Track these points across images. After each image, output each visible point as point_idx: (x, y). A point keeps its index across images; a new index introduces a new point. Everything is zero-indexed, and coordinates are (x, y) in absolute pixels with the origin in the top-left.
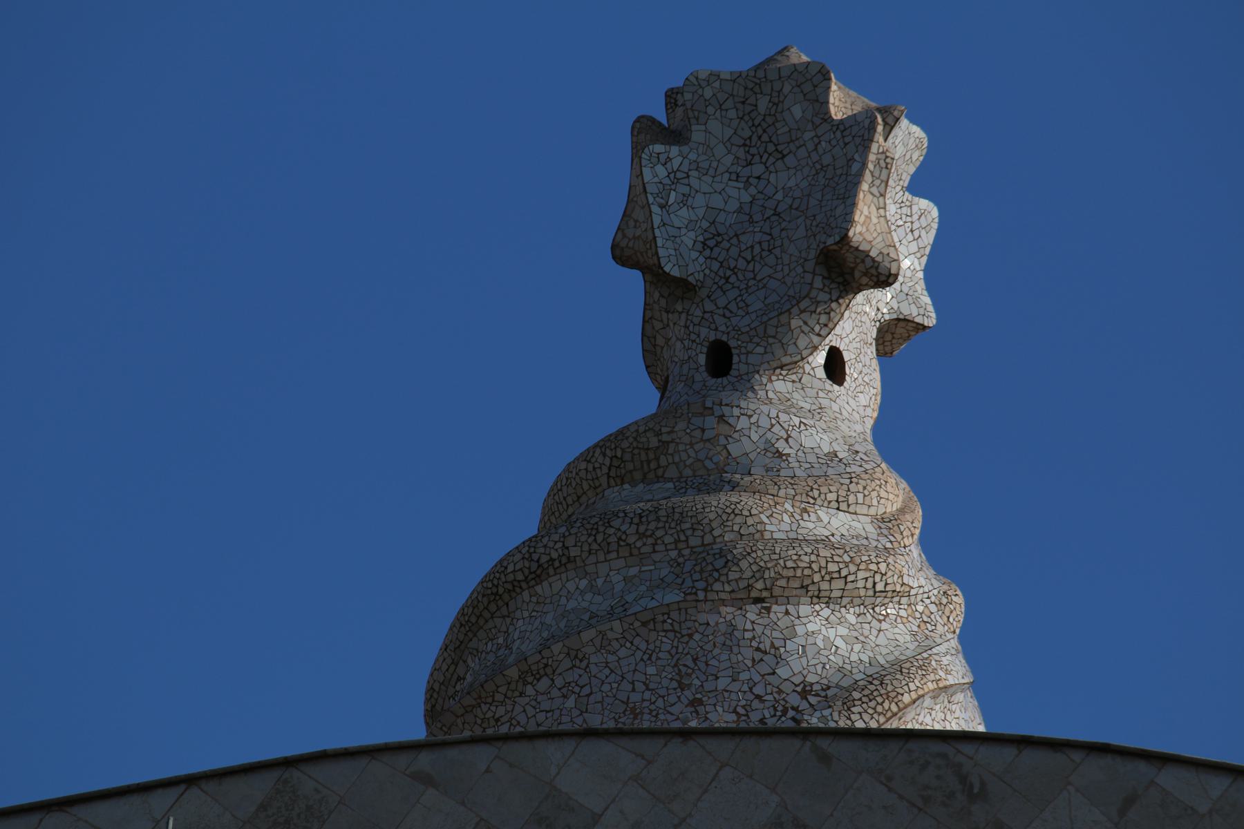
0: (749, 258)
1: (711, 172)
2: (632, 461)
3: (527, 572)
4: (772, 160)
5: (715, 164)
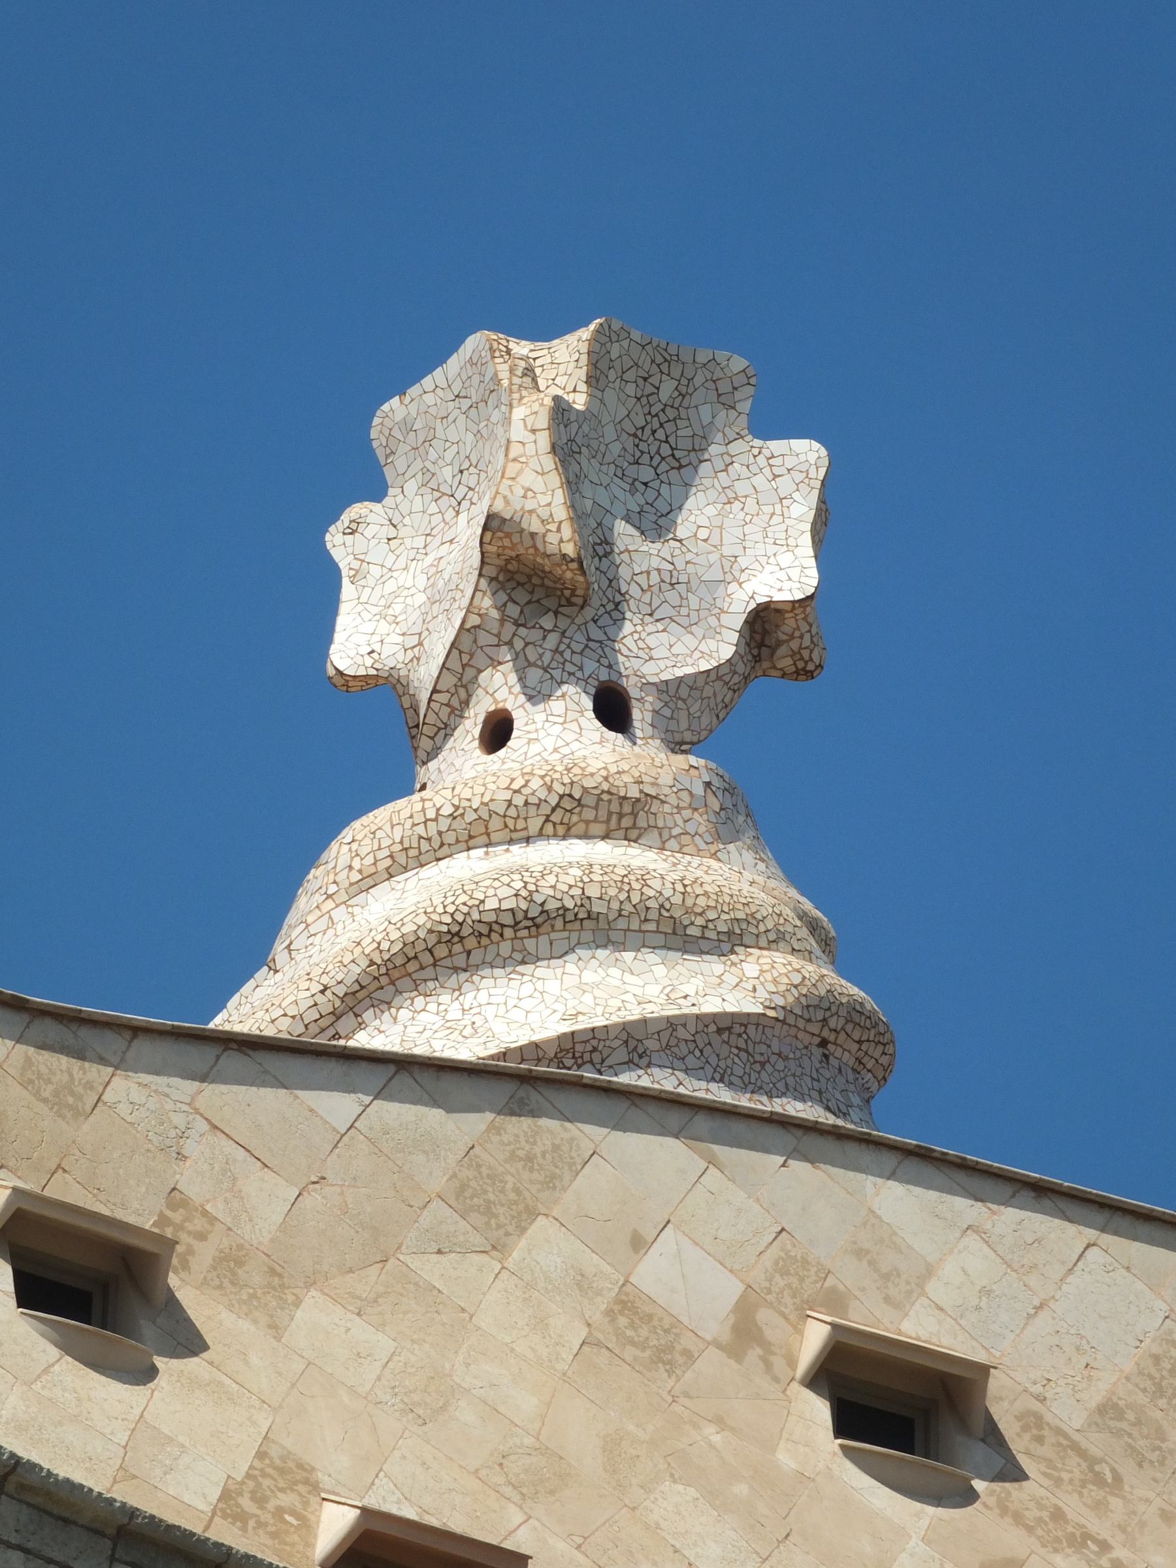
1: (599, 456)
2: (596, 808)
3: (520, 916)
4: (664, 467)
5: (603, 448)
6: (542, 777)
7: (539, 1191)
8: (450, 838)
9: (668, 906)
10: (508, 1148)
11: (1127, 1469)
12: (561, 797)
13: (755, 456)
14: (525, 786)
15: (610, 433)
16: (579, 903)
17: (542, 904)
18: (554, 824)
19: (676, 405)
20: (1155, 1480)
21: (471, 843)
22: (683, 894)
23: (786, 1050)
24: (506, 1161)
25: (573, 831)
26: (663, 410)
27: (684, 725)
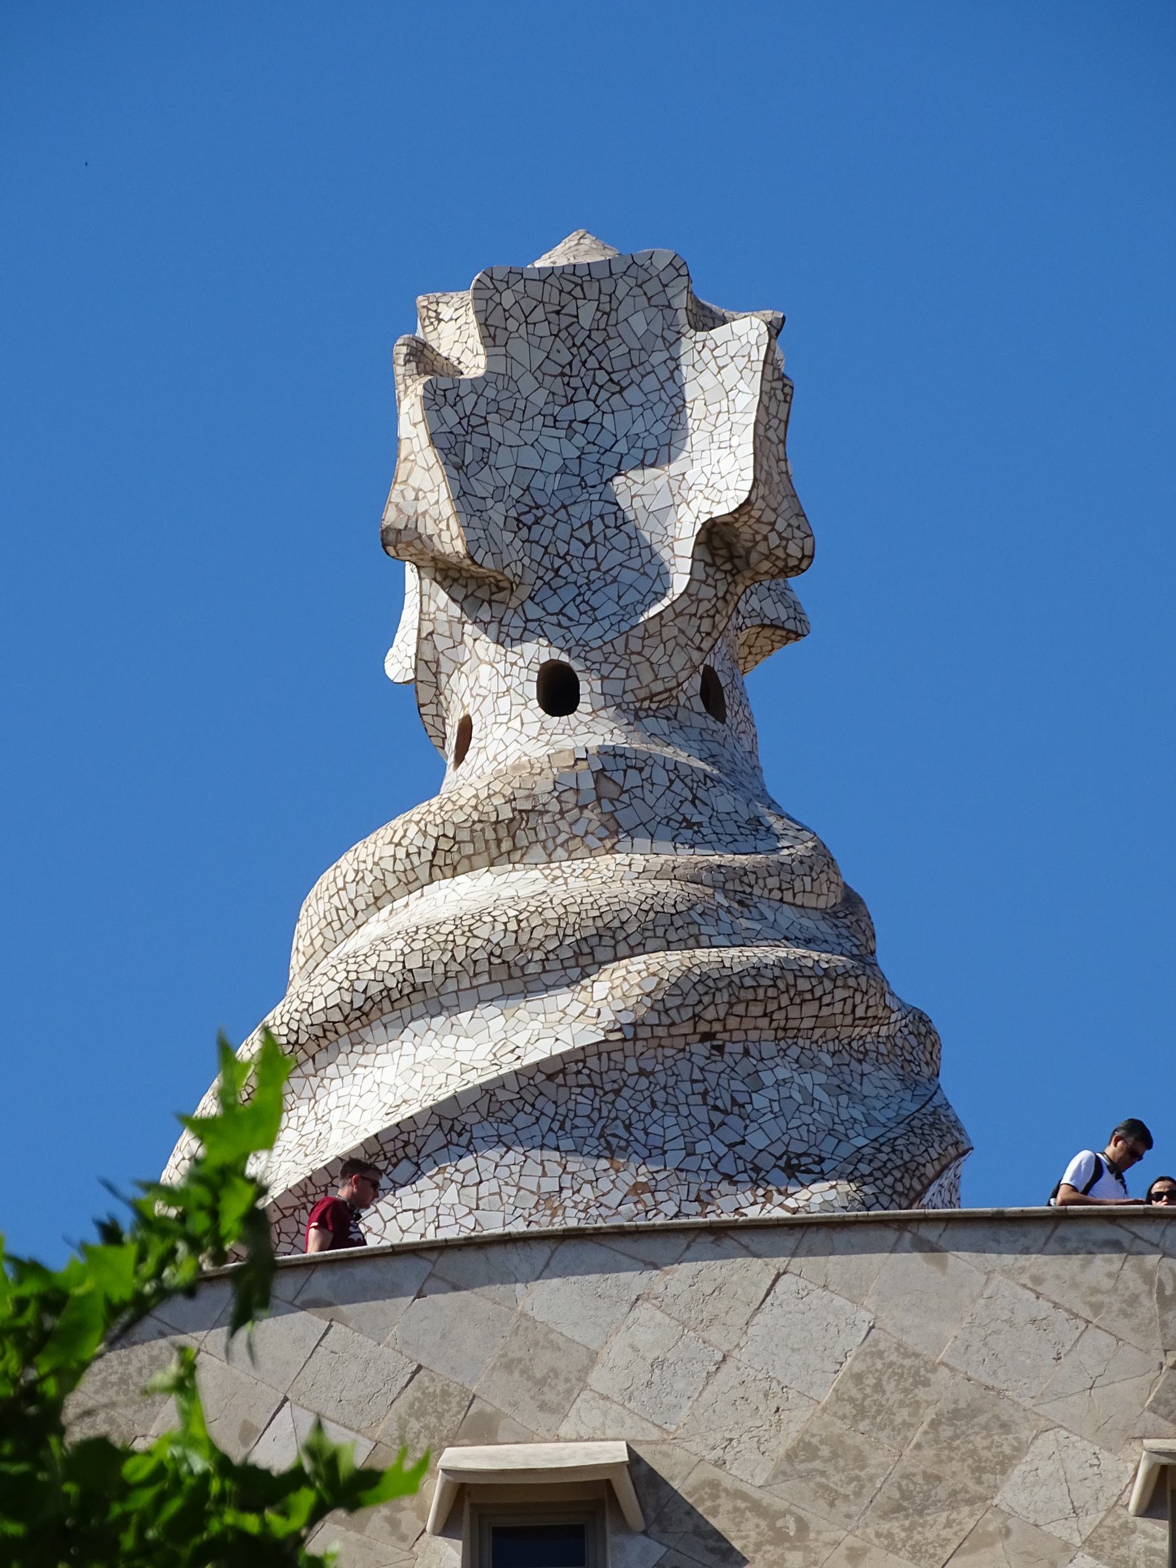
0: (588, 541)
1: (518, 415)
4: (604, 395)
5: (521, 404)
6: (417, 823)
7: (135, 1412)
8: (360, 905)
9: (497, 952)
10: (99, 1377)
11: (815, 1513)
12: (437, 839)
13: (699, 352)
14: (404, 836)
15: (527, 384)
16: (401, 979)
17: (365, 991)
18: (440, 867)
19: (602, 326)
20: (848, 1516)
21: (379, 904)
22: (516, 932)
23: (648, 1066)
24: (97, 1392)
25: (459, 868)
26: (589, 337)
27: (647, 677)
